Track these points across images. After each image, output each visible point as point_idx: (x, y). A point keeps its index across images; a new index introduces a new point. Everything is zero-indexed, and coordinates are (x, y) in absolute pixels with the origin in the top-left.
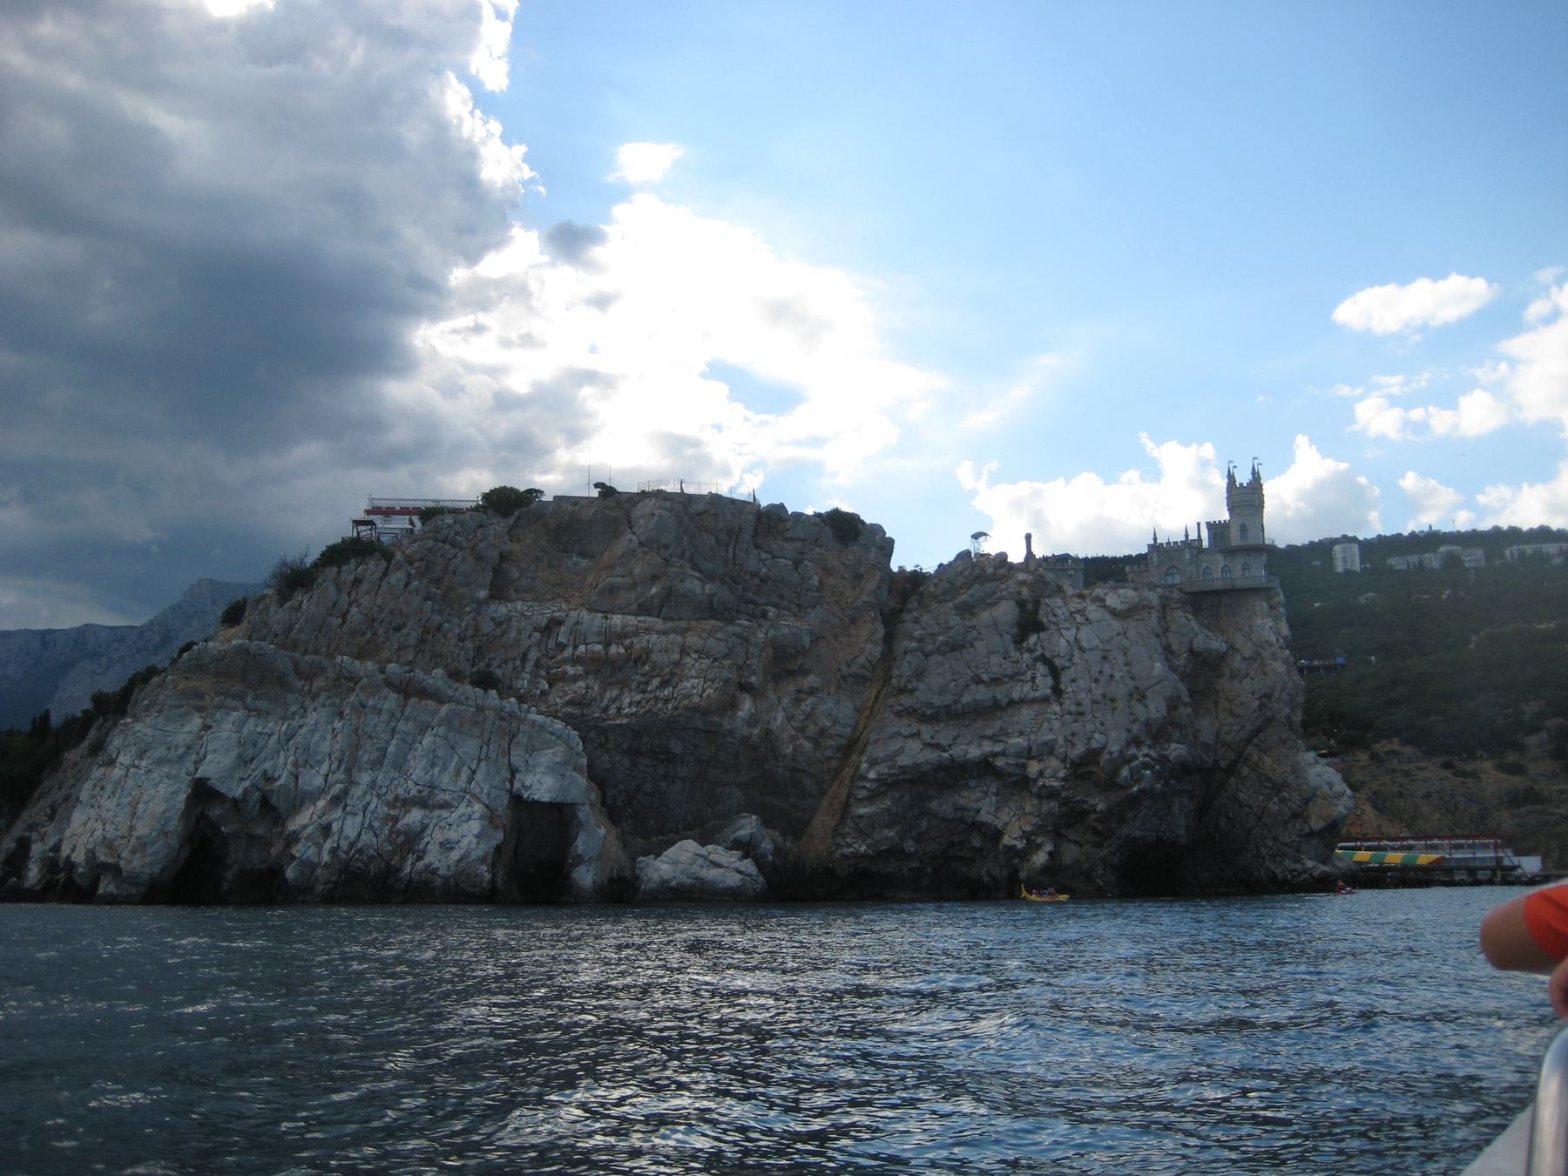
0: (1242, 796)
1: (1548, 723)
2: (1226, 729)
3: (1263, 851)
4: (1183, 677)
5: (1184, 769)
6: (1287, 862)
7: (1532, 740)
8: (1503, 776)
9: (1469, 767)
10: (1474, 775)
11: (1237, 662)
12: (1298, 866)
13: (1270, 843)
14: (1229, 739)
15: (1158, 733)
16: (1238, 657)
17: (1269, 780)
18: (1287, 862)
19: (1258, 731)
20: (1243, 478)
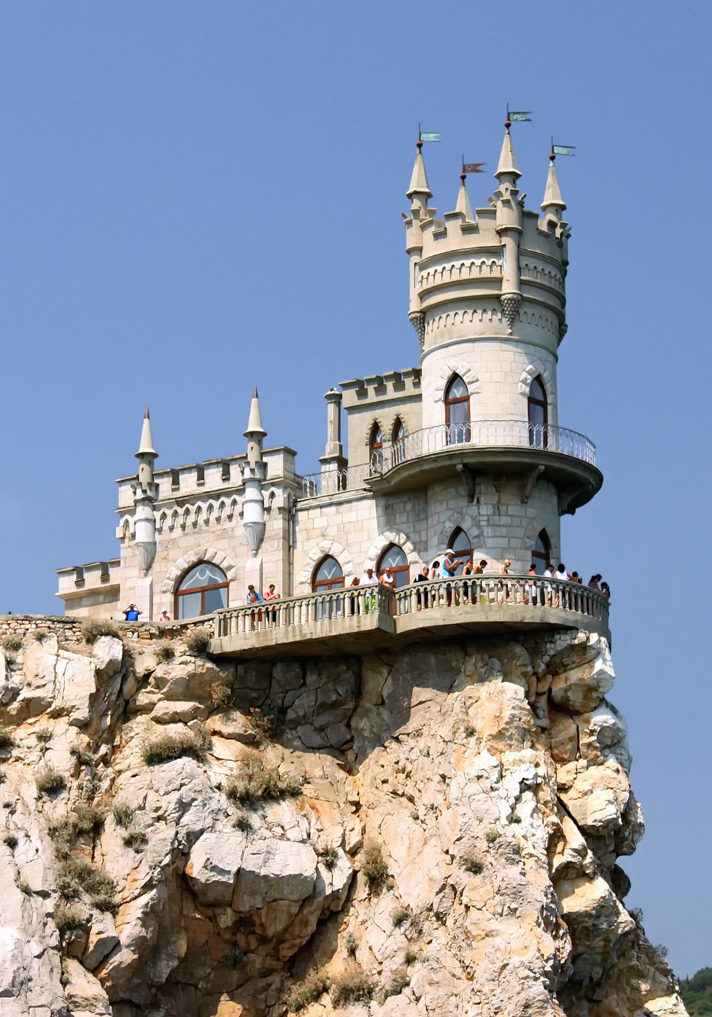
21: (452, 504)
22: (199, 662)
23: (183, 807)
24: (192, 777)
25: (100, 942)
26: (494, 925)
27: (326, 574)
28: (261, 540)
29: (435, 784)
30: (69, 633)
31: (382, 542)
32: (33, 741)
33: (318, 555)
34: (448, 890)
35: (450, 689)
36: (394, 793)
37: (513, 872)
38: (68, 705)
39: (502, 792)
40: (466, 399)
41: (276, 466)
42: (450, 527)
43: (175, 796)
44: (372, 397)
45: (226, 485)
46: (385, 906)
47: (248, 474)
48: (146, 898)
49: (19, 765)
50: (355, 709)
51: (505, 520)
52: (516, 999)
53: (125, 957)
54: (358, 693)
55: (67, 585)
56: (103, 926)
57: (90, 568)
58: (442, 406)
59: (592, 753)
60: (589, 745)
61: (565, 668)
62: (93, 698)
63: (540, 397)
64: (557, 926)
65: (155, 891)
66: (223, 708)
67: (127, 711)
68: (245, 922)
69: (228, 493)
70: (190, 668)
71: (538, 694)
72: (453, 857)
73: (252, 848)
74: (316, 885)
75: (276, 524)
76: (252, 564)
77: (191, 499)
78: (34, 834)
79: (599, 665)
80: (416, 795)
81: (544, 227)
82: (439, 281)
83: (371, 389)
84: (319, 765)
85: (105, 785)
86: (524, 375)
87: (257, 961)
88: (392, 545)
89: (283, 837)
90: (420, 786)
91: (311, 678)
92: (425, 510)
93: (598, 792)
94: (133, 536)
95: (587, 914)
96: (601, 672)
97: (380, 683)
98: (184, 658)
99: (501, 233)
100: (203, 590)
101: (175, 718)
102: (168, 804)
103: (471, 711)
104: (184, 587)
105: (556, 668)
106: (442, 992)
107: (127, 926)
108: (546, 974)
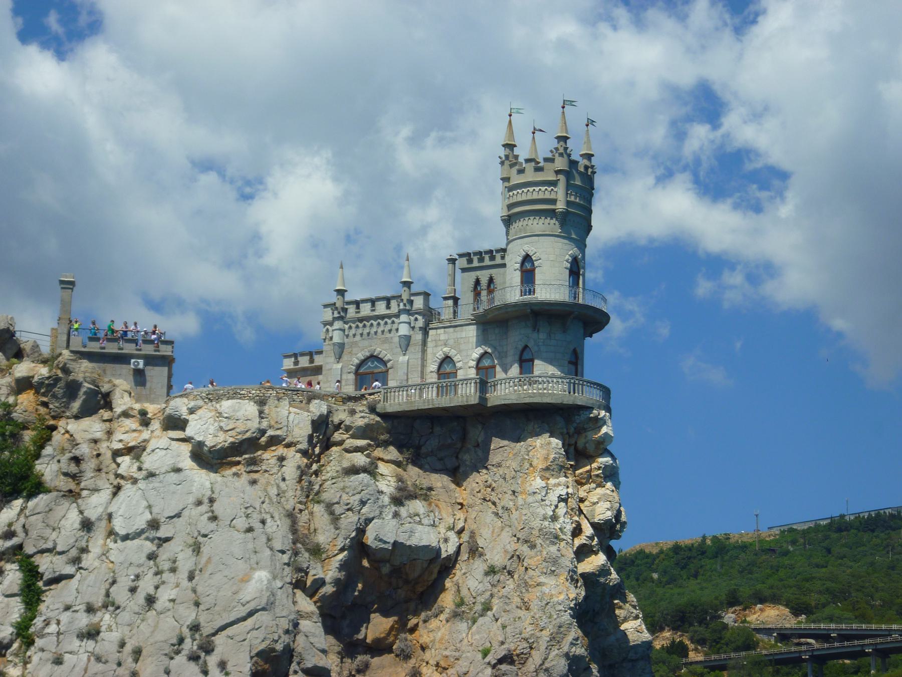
11: (468, 579)
22: (372, 416)
23: (363, 503)
24: (368, 486)
25: (315, 581)
26: (542, 579)
27: (448, 369)
28: (408, 345)
29: (509, 496)
30: (295, 397)
31: (480, 350)
32: (273, 461)
33: (440, 355)
34: (515, 558)
35: (518, 440)
36: (484, 499)
37: (553, 549)
38: (295, 440)
39: (547, 502)
41: (419, 303)
43: (358, 497)
44: (476, 264)
45: (388, 312)
46: (479, 566)
47: (402, 306)
49: (266, 475)
50: (461, 449)
52: (554, 622)
53: (328, 589)
54: (464, 438)
55: (288, 364)
56: (316, 571)
57: (303, 355)
58: (518, 273)
59: (599, 480)
60: (597, 476)
61: (585, 430)
62: (310, 437)
63: (575, 269)
64: (577, 581)
65: (346, 552)
66: (385, 444)
67: (327, 445)
69: (389, 316)
70: (366, 420)
71: (569, 445)
72: (518, 539)
73: (402, 529)
74: (438, 551)
75: (418, 337)
76: (403, 359)
77: (368, 319)
78: (277, 517)
79: (604, 430)
80: (497, 501)
81: (582, 170)
82: (519, 199)
83: (475, 259)
84: (440, 481)
85: (316, 487)
86: (567, 257)
88: (486, 353)
89: (420, 523)
90: (500, 496)
91: (437, 430)
93: (601, 503)
94: (331, 338)
95: (593, 574)
96: (606, 434)
97: (476, 433)
98: (363, 414)
99: (558, 172)
101: (357, 449)
102: (355, 500)
103: (531, 453)
105: (580, 431)
106: (511, 616)
107: (329, 571)
108: (571, 608)
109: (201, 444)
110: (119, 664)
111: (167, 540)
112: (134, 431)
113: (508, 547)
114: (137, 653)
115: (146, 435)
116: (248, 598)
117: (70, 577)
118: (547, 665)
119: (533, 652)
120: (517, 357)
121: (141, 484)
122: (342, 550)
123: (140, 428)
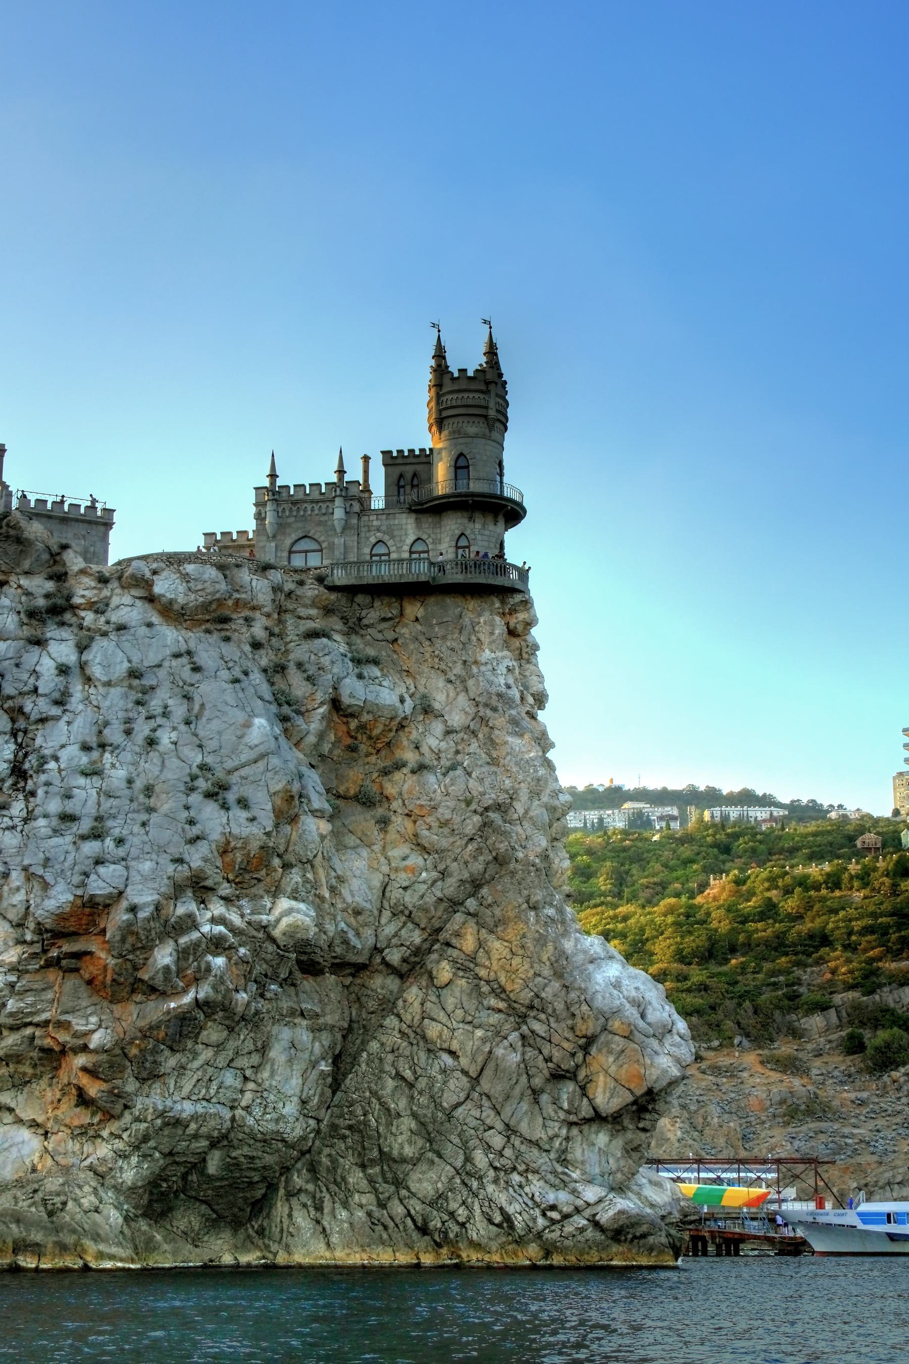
0: (433, 1030)
1: (838, 999)
2: (403, 878)
3: (481, 1159)
4: (319, 760)
5: (307, 960)
6: (536, 1186)
7: (816, 1022)
8: (775, 1076)
9: (724, 1060)
10: (731, 1072)
12: (562, 1197)
13: (497, 1141)
14: (410, 899)
15: (251, 871)
16: (438, 728)
17: (500, 992)
18: (536, 1186)
19: (476, 885)
20: (467, 358)
21: (459, 521)
34: (477, 719)
40: (467, 467)
42: (458, 532)
48: (321, 710)
51: (487, 532)
54: (402, 614)
65: (325, 707)
68: (362, 727)
87: (363, 748)
91: (377, 604)
92: (440, 522)
100: (306, 552)
101: (309, 618)
104: (294, 549)
105: (513, 611)
109: (171, 602)
110: (132, 801)
111: (153, 688)
112: (95, 588)
113: (468, 709)
114: (149, 790)
115: (106, 593)
116: (256, 742)
117: (57, 718)
118: (531, 814)
119: (514, 803)
120: (454, 543)
121: (113, 636)
122: (322, 704)
123: (99, 586)
